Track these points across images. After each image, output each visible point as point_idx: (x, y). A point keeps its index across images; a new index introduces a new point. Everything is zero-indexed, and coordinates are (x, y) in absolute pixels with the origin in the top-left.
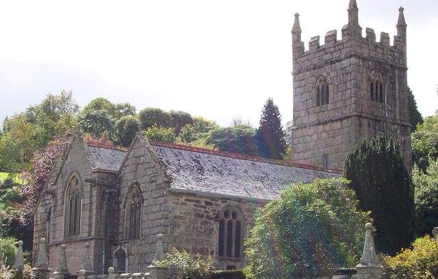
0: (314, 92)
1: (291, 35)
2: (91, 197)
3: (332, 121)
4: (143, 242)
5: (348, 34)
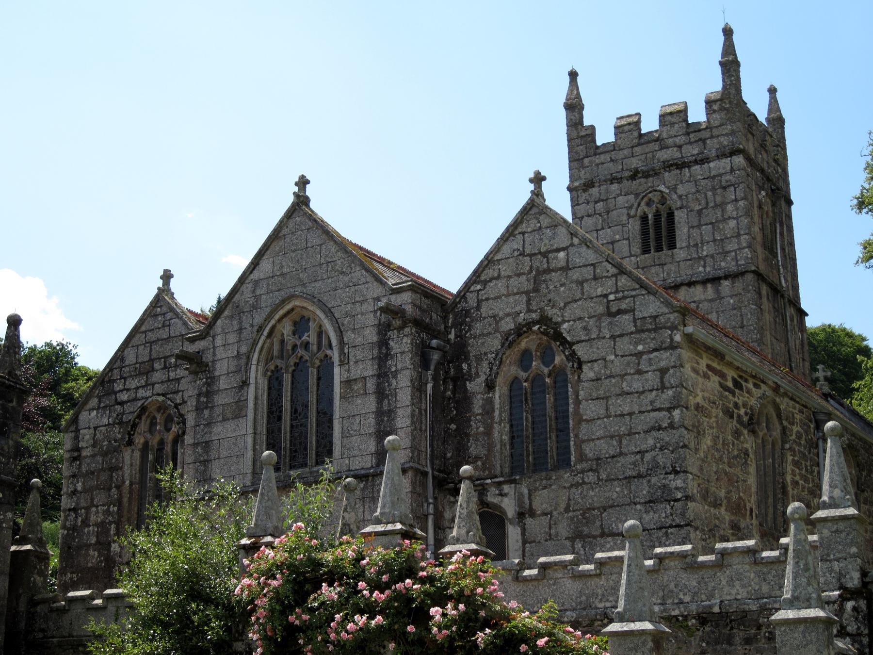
0: (635, 226)
1: (563, 113)
3: (690, 284)
4: (591, 477)
5: (722, 109)
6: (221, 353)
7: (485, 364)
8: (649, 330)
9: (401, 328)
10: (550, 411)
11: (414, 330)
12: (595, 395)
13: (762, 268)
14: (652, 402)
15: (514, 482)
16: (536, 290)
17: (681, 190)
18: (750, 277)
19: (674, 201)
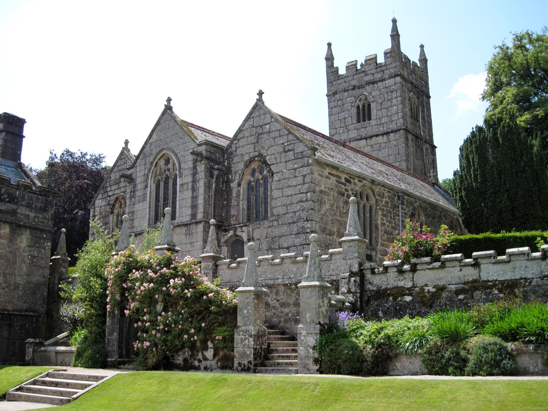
0: (354, 111)
1: (325, 61)
2: (195, 174)
3: (377, 136)
4: (275, 223)
5: (391, 56)
6: (139, 174)
7: (238, 175)
8: (299, 158)
9: (201, 161)
10: (262, 195)
11: (206, 161)
12: (278, 187)
13: (410, 127)
14: (299, 190)
15: (246, 226)
16: (258, 142)
17: (374, 94)
18: (402, 131)
19: (370, 99)
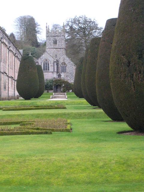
0: (53, 41)
